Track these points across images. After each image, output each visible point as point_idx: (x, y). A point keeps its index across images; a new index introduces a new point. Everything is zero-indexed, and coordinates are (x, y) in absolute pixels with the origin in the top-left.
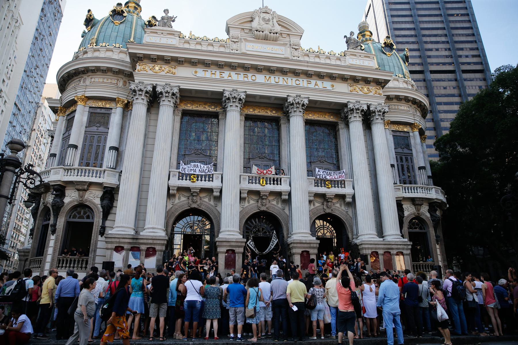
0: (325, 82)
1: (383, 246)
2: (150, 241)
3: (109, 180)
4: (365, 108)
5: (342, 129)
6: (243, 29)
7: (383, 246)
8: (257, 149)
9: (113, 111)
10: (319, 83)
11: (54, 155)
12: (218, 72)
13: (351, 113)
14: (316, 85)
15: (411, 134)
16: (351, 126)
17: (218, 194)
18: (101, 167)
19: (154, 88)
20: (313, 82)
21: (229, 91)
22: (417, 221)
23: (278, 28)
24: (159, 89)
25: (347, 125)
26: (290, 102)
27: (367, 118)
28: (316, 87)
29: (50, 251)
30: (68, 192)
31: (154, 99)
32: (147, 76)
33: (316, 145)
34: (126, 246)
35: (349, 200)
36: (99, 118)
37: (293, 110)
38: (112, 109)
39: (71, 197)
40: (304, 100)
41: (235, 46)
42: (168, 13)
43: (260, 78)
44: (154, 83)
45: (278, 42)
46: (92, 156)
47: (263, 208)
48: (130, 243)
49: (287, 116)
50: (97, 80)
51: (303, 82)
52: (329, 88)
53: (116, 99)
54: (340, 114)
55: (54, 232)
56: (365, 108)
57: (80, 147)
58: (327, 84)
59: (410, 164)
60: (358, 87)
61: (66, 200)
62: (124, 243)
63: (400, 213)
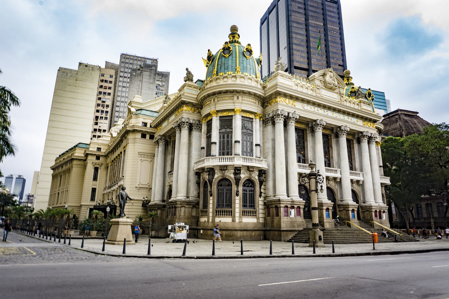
2: (298, 203)
4: (370, 135)
6: (321, 81)
9: (254, 120)
10: (352, 118)
12: (313, 107)
18: (253, 156)
19: (288, 114)
20: (350, 118)
24: (291, 115)
29: (237, 206)
30: (242, 171)
32: (283, 106)
34: (289, 206)
35: (361, 183)
38: (252, 119)
39: (244, 176)
41: (318, 91)
43: (330, 113)
44: (289, 111)
45: (335, 91)
48: (291, 204)
50: (245, 99)
52: (356, 122)
53: (256, 113)
55: (237, 195)
58: (354, 120)
60: (366, 123)
61: (242, 176)
62: (288, 204)
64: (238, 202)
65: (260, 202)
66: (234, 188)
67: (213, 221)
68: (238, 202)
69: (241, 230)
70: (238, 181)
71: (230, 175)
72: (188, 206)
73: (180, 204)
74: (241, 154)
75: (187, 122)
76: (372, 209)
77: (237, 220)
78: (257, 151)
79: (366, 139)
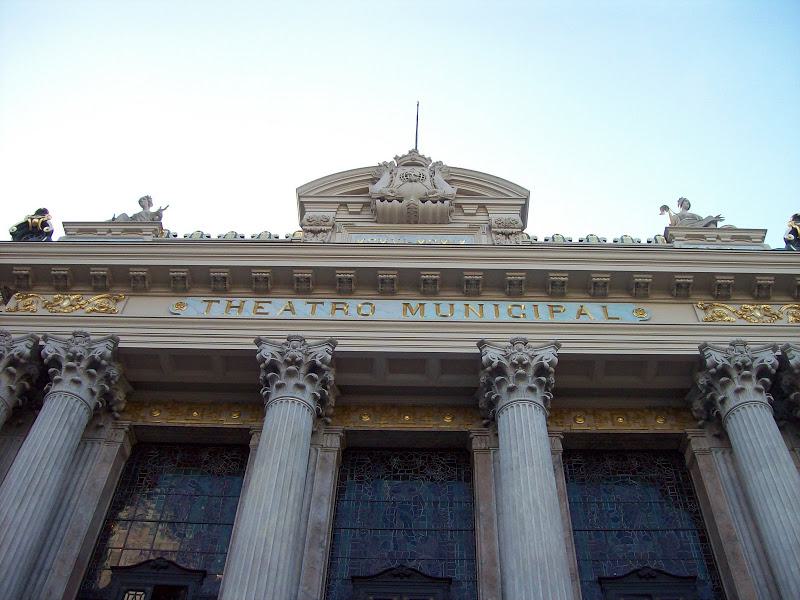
0: (610, 306)
5: (705, 452)
6: (344, 204)
8: (385, 545)
12: (250, 303)
13: (724, 385)
14: (581, 313)
16: (735, 427)
21: (274, 344)
23: (449, 190)
24: (49, 350)
25: (723, 437)
26: (490, 363)
28: (583, 319)
33: (615, 520)
37: (504, 389)
40: (541, 353)
42: (150, 204)
43: (389, 309)
49: (489, 418)
51: (535, 311)
54: (688, 408)
79: (750, 387)
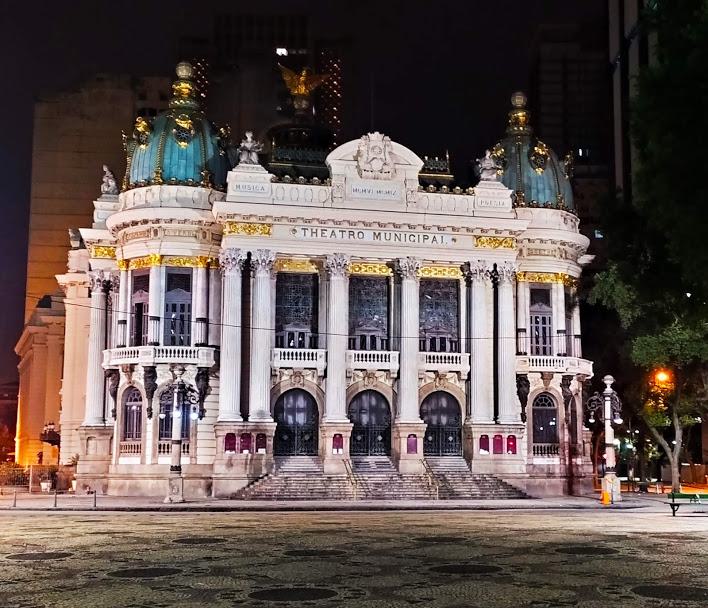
1: (494, 430)
3: (204, 359)
7: (494, 430)
11: (124, 322)
15: (554, 287)
17: (322, 374)
22: (544, 398)
27: (495, 278)
31: (247, 269)
36: (179, 280)
39: (163, 379)
46: (178, 330)
47: (371, 387)
55: (150, 416)
56: (491, 269)
57: (162, 316)
59: (547, 326)
61: (159, 382)
63: (525, 389)
64: (150, 427)
65: (202, 428)
66: (145, 403)
67: (117, 460)
68: (150, 427)
69: (152, 478)
70: (151, 388)
71: (139, 378)
72: (101, 438)
73: (86, 434)
74: (161, 342)
75: (99, 280)
76: (471, 433)
77: (149, 461)
78: (197, 332)
